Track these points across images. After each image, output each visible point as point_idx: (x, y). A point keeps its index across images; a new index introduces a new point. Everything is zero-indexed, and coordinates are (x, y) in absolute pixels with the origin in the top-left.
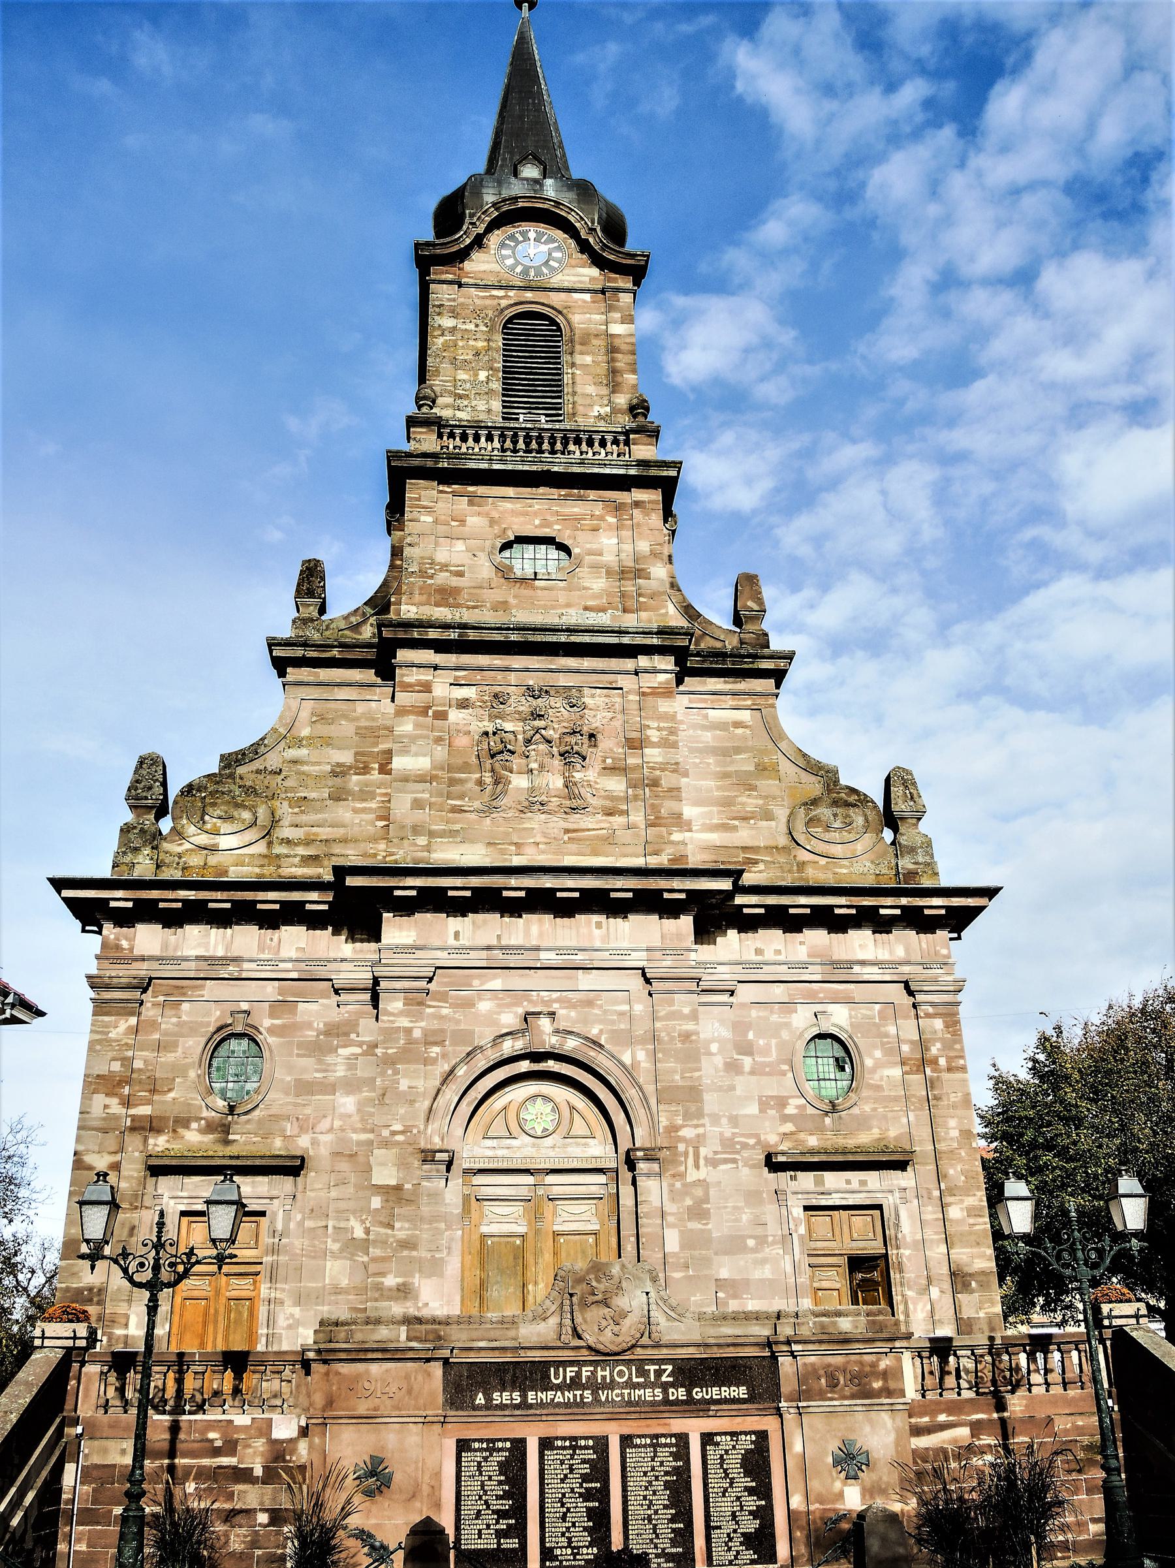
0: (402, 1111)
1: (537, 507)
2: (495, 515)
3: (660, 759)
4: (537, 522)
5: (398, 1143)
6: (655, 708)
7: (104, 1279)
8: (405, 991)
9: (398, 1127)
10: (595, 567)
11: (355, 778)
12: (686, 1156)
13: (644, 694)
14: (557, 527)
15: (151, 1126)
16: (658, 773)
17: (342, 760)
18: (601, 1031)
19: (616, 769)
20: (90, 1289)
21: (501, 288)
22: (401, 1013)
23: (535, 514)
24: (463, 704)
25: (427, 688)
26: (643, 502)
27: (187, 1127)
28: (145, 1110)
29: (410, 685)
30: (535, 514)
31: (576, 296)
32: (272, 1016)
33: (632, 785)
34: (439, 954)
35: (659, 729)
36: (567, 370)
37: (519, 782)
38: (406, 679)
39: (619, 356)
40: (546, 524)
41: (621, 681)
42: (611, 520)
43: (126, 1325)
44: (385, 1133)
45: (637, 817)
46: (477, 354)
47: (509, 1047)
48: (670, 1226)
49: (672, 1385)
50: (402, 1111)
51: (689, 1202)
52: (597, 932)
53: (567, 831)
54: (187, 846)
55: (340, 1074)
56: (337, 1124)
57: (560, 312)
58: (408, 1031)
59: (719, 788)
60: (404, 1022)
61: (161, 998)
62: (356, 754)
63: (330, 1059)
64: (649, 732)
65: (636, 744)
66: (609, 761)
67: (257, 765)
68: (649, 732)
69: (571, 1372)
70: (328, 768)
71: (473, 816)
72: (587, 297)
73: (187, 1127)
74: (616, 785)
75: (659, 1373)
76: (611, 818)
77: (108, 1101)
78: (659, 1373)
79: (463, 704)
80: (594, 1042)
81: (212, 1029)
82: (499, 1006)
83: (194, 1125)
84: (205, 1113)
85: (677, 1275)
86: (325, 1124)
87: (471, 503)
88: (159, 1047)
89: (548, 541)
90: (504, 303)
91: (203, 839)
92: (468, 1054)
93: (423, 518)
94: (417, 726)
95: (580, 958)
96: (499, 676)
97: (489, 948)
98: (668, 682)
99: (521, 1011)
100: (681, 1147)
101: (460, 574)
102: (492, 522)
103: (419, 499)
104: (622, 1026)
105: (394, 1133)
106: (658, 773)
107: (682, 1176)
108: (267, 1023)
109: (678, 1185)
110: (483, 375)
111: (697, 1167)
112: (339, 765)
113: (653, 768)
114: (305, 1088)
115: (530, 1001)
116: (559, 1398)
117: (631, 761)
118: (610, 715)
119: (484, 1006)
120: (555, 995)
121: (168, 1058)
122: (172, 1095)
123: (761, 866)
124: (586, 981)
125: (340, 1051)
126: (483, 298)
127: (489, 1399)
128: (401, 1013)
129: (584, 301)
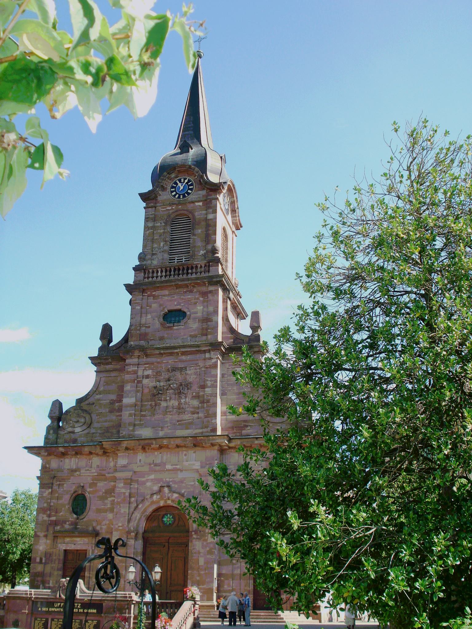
2: (162, 302)
3: (210, 392)
4: (176, 303)
5: (120, 530)
6: (210, 372)
7: (42, 570)
9: (120, 525)
10: (194, 319)
11: (117, 404)
13: (207, 368)
14: (182, 304)
15: (55, 523)
17: (112, 398)
18: (185, 492)
19: (197, 397)
20: (39, 573)
22: (123, 487)
23: (175, 300)
24: (147, 377)
25: (135, 372)
27: (66, 523)
28: (54, 518)
30: (175, 300)
31: (197, 204)
32: (90, 488)
35: (211, 381)
37: (164, 404)
38: (129, 370)
40: (179, 304)
42: (201, 299)
43: (49, 584)
44: (117, 526)
46: (160, 236)
48: (201, 556)
49: (80, 608)
51: (208, 549)
52: (184, 457)
53: (178, 421)
54: (66, 432)
55: (109, 506)
56: (107, 522)
58: (124, 493)
59: (237, 399)
60: (123, 490)
61: (58, 483)
62: (117, 396)
63: (106, 501)
64: (207, 382)
65: (203, 387)
66: (194, 394)
67: (87, 402)
68: (207, 382)
69: (59, 604)
70: (109, 401)
71: (148, 418)
72: (201, 204)
73: (66, 523)
74: (195, 403)
75: (77, 606)
76: (194, 415)
77: (43, 516)
78: (77, 606)
79: (147, 377)
81: (72, 492)
82: (153, 484)
83: (67, 523)
84: (71, 519)
85: (202, 572)
86: (104, 522)
87: (154, 299)
88: (58, 498)
90: (171, 211)
91: (70, 429)
92: (142, 500)
93: (137, 307)
94: (131, 387)
97: (150, 464)
99: (160, 485)
101: (149, 327)
102: (161, 305)
103: (136, 300)
105: (119, 526)
107: (206, 540)
108: (88, 490)
109: (205, 543)
110: (162, 244)
112: (112, 400)
114: (99, 511)
116: (56, 610)
117: (201, 393)
119: (149, 484)
121: (60, 502)
122: (61, 513)
123: (249, 428)
125: (109, 499)
127: (41, 609)
128: (123, 487)
129: (200, 206)
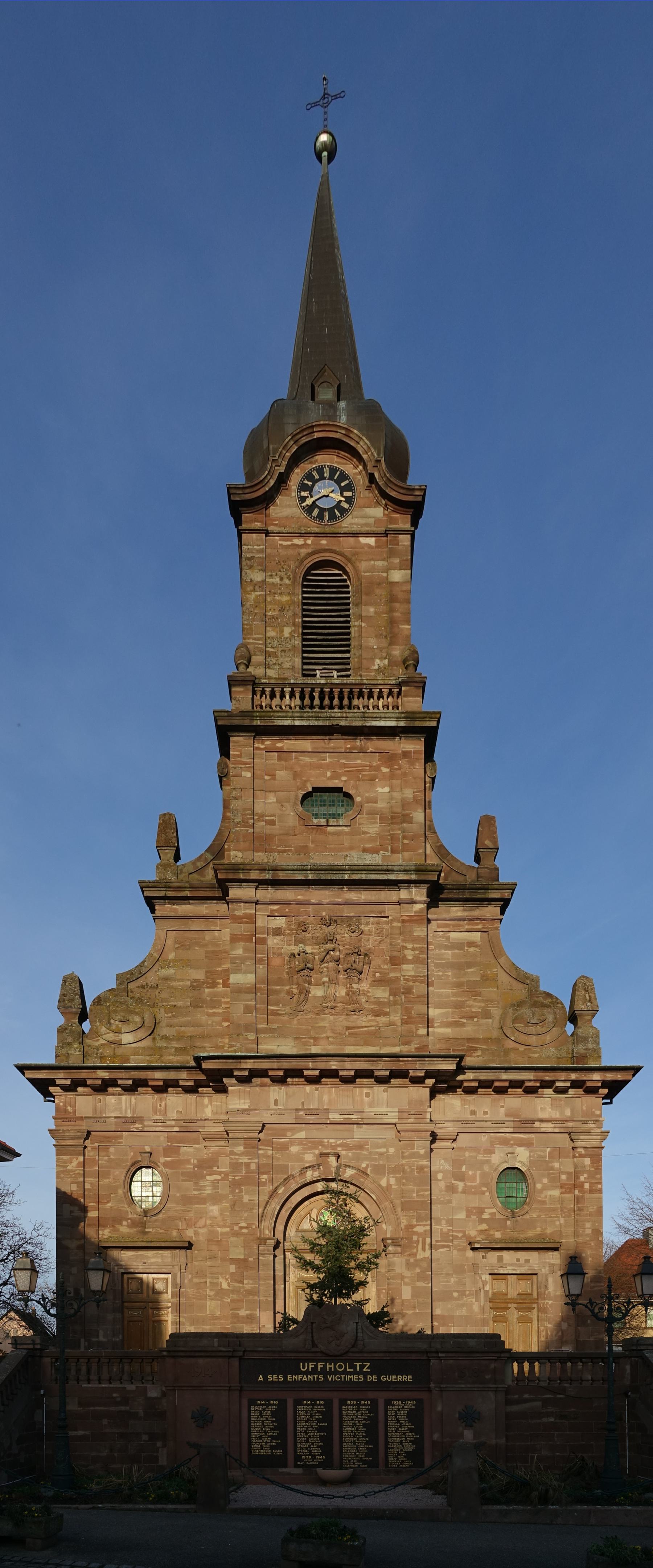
0: (245, 1215)
1: (328, 760)
8: (246, 1139)
12: (418, 1242)
14: (344, 778)
16: (411, 983)
18: (368, 1165)
21: (301, 535)
26: (410, 752)
29: (240, 917)
31: (363, 540)
33: (393, 993)
34: (265, 1114)
35: (413, 949)
36: (354, 623)
38: (237, 913)
39: (397, 605)
41: (390, 911)
45: (396, 1018)
47: (310, 1175)
50: (245, 1215)
51: (418, 1270)
53: (348, 1028)
57: (349, 560)
64: (407, 952)
68: (407, 952)
71: (285, 1018)
72: (371, 541)
76: (378, 1019)
80: (363, 1172)
87: (279, 759)
89: (339, 790)
90: (304, 551)
95: (354, 1117)
96: (302, 908)
97: (297, 1111)
98: (421, 910)
100: (415, 1238)
102: (296, 775)
104: (381, 1162)
106: (411, 983)
107: (414, 1255)
109: (412, 1260)
111: (424, 1249)
113: (407, 980)
115: (323, 1146)
117: (393, 975)
118: (379, 938)
120: (339, 1142)
124: (359, 1133)
126: (287, 547)
